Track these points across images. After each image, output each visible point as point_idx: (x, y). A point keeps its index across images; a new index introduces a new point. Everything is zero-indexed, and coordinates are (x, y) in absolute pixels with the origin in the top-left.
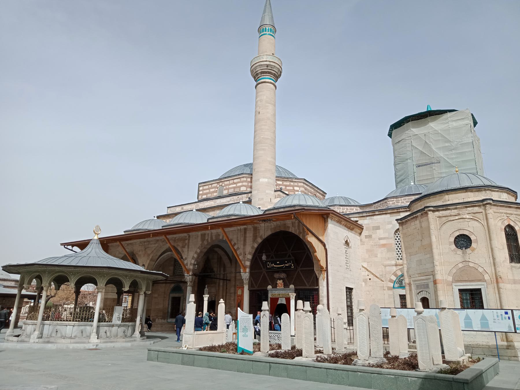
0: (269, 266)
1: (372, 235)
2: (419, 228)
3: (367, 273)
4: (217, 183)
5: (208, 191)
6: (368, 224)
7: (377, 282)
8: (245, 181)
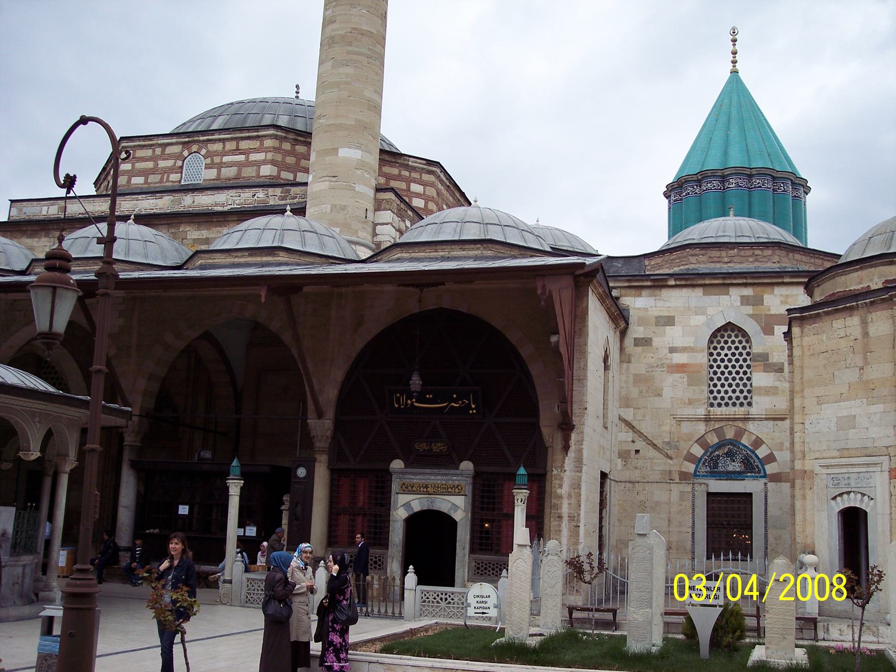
0: (398, 402)
1: (653, 339)
2: (859, 337)
3: (630, 436)
4: (184, 143)
5: (150, 165)
6: (646, 309)
8: (276, 150)
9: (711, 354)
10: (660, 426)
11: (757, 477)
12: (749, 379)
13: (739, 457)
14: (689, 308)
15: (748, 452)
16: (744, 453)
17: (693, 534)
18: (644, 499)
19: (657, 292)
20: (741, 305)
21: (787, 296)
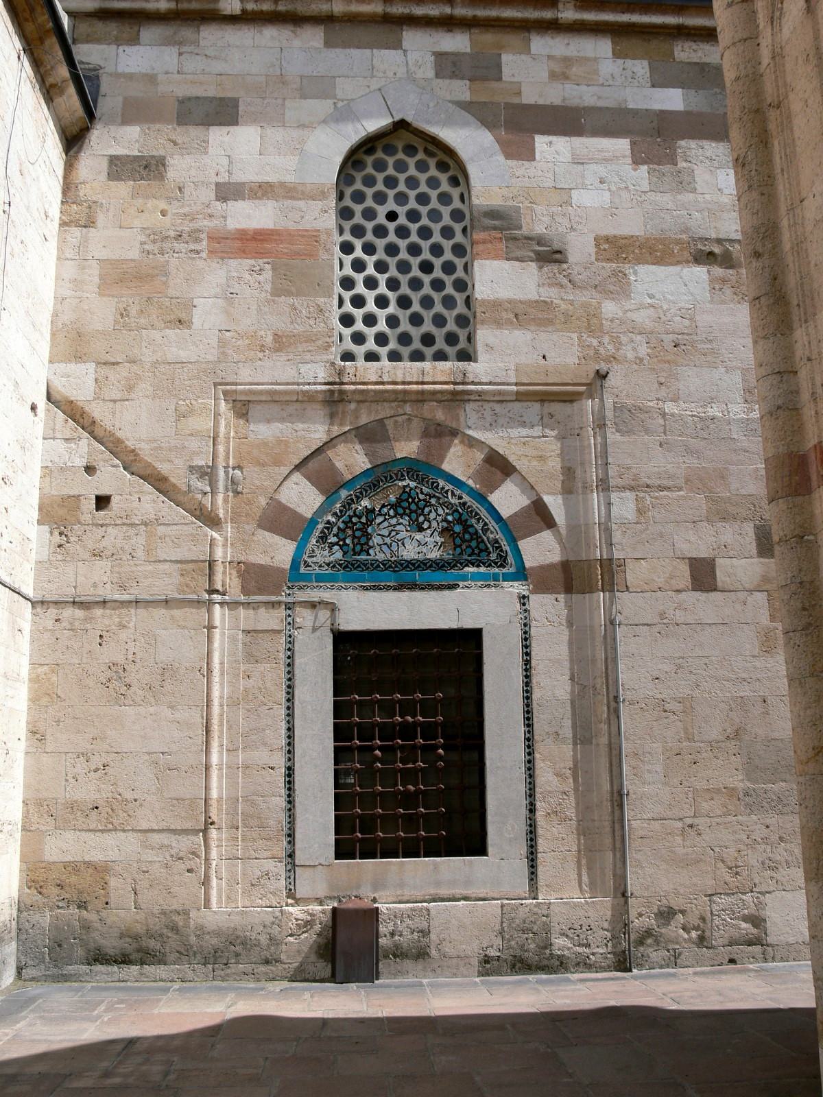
1: (169, 161)
6: (151, 79)
7: (161, 530)
9: (345, 214)
10: (181, 416)
11: (495, 578)
12: (461, 285)
13: (437, 516)
14: (282, 80)
15: (466, 498)
16: (454, 501)
17: (290, 773)
18: (120, 659)
19: (187, 32)
20: (437, 76)
21: (567, 61)
